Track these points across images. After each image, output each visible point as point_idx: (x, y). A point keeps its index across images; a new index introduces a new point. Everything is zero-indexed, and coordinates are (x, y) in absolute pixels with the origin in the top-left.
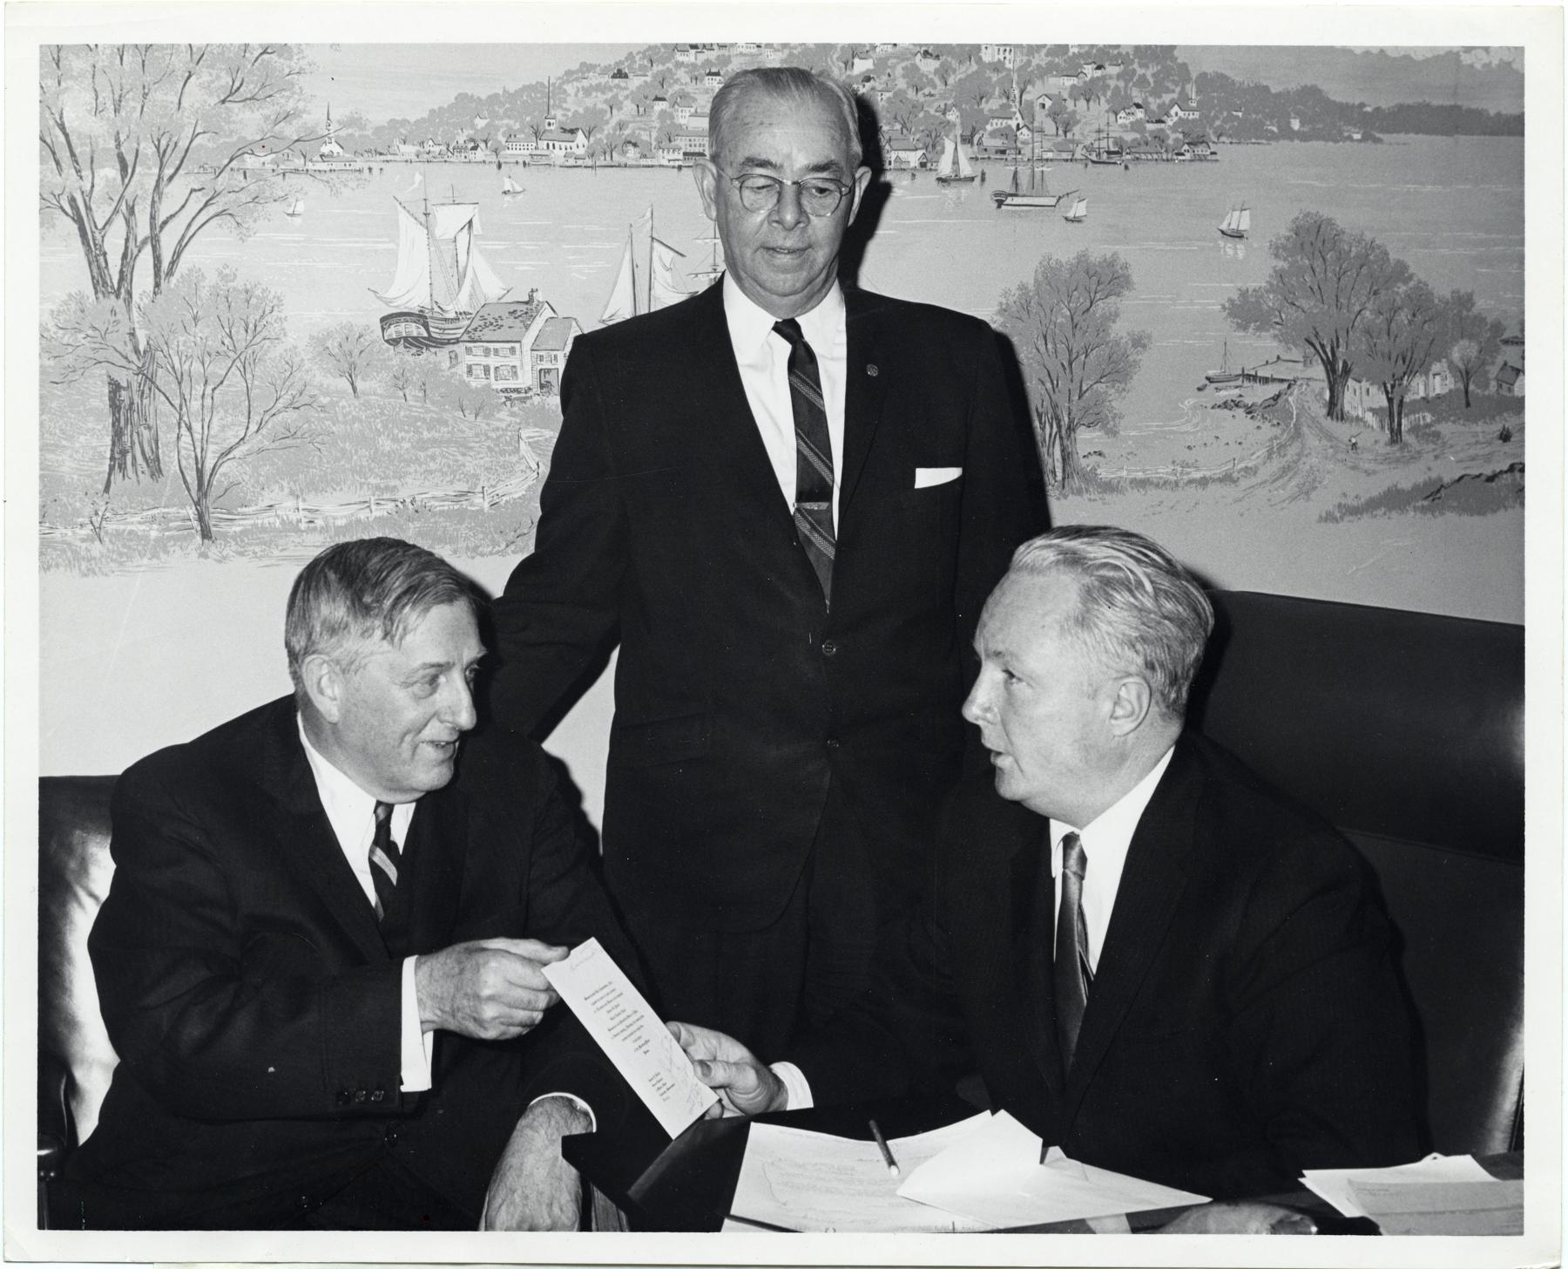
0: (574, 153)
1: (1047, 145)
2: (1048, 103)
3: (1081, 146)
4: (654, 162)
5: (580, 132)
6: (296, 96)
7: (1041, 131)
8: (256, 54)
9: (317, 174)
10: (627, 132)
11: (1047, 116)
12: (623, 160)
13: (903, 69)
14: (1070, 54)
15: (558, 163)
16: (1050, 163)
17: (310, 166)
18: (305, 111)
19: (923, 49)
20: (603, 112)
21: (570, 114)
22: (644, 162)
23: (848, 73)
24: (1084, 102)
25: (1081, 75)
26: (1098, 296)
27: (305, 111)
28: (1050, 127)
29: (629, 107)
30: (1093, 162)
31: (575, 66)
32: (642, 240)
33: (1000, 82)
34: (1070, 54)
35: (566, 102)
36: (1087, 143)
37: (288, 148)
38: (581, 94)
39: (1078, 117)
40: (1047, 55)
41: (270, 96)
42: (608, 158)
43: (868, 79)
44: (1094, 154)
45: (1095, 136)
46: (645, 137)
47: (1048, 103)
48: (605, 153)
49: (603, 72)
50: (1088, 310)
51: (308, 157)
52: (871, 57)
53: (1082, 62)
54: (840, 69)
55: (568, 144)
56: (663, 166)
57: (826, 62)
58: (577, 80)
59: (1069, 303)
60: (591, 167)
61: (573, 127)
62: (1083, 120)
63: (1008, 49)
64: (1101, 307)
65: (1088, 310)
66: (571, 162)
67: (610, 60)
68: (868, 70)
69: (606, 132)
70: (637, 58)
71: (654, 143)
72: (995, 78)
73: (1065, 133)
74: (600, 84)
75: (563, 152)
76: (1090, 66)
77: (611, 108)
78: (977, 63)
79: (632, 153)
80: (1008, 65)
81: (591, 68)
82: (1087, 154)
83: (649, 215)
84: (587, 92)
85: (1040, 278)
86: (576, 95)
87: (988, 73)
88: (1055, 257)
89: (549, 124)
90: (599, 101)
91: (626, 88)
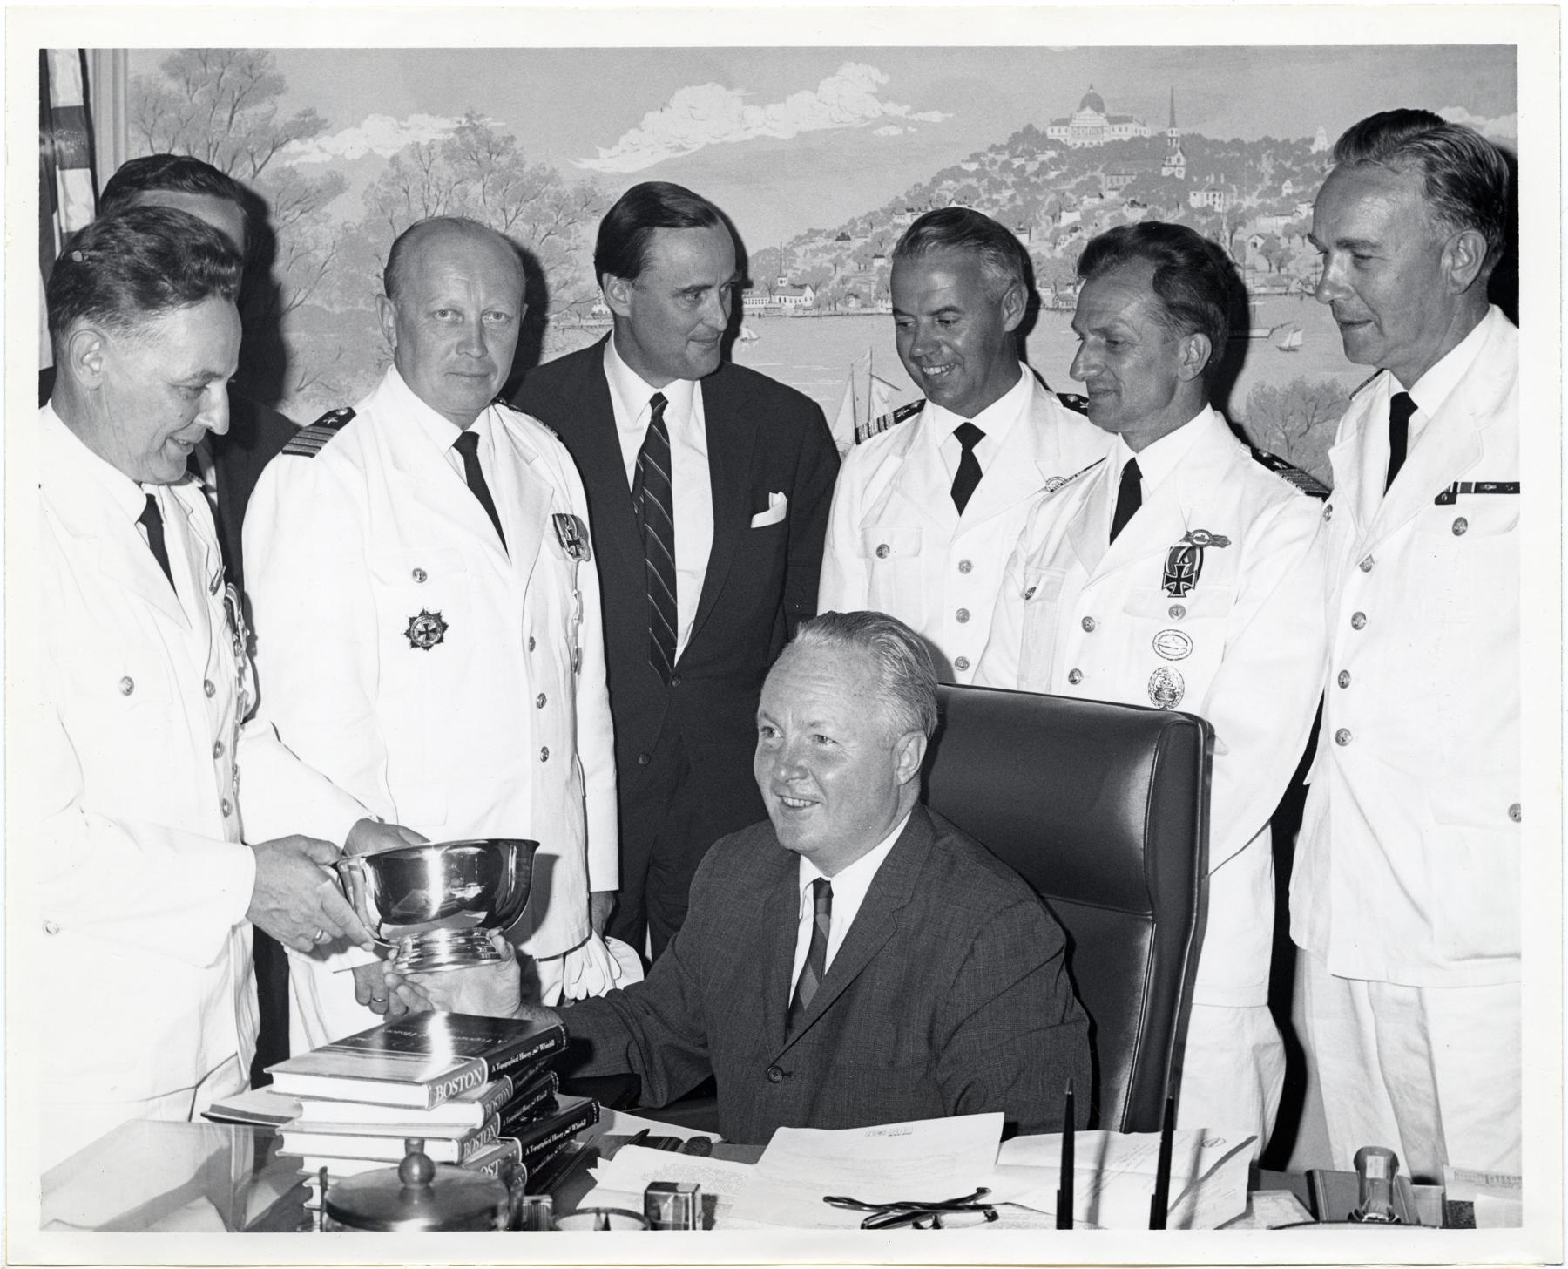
0: (802, 306)
1: (1259, 281)
2: (1260, 242)
3: (1296, 281)
4: (873, 311)
5: (808, 288)
6: (573, 268)
7: (1253, 268)
8: (542, 236)
9: (590, 330)
10: (850, 286)
11: (1261, 253)
12: (846, 310)
13: (1110, 218)
14: (1284, 194)
15: (789, 314)
16: (1262, 298)
17: (584, 323)
18: (579, 279)
19: (1133, 198)
20: (829, 270)
21: (799, 273)
22: (863, 311)
23: (1056, 225)
24: (1301, 239)
25: (1296, 214)
26: (1316, 420)
27: (579, 279)
28: (1262, 264)
29: (851, 265)
30: (1310, 295)
31: (803, 232)
32: (861, 375)
33: (1208, 223)
34: (1284, 194)
35: (794, 261)
36: (1303, 277)
37: (567, 309)
38: (809, 254)
39: (1292, 253)
40: (1259, 197)
41: (553, 268)
42: (833, 308)
43: (1075, 229)
44: (1311, 287)
45: (1312, 270)
46: (865, 290)
47: (1260, 242)
48: (830, 304)
49: (829, 236)
50: (1305, 433)
51: (583, 314)
52: (1077, 209)
53: (1297, 202)
54: (1048, 224)
55: (798, 298)
56: (879, 314)
57: (1035, 216)
58: (805, 243)
59: (1284, 427)
60: (817, 316)
61: (804, 282)
62: (1299, 256)
63: (1217, 194)
64: (1317, 431)
65: (1305, 433)
66: (800, 313)
67: (835, 223)
68: (1075, 222)
69: (830, 287)
70: (859, 223)
71: (873, 295)
72: (1203, 221)
73: (1279, 269)
74: (825, 247)
75: (793, 305)
76: (1305, 206)
77: (835, 266)
78: (1184, 207)
79: (853, 303)
80: (1217, 209)
81: (819, 233)
82: (1303, 288)
83: (868, 355)
84: (815, 253)
85: (1252, 403)
86: (806, 251)
87: (1197, 217)
88: (1268, 383)
89: (781, 282)
90: (824, 260)
91: (849, 249)
